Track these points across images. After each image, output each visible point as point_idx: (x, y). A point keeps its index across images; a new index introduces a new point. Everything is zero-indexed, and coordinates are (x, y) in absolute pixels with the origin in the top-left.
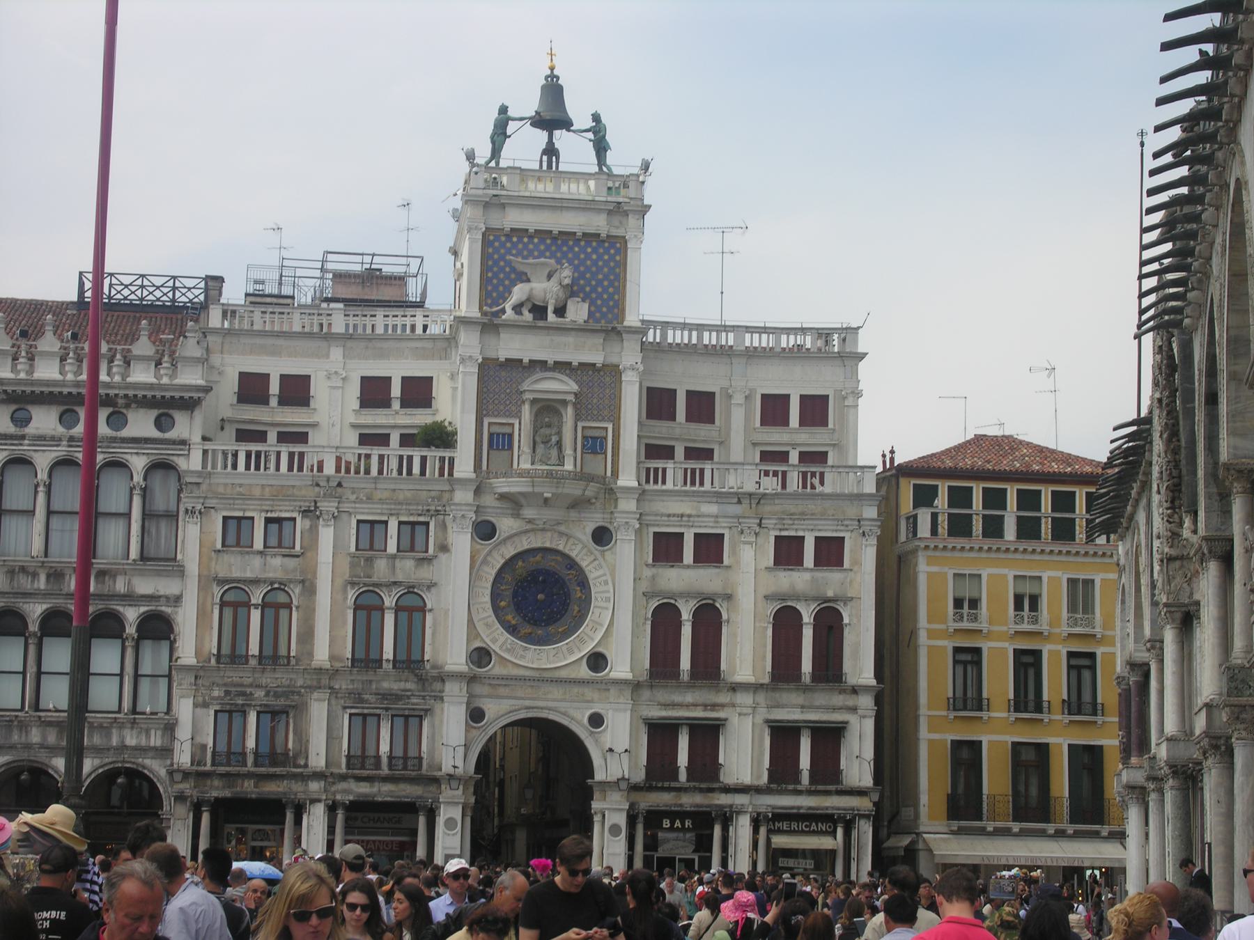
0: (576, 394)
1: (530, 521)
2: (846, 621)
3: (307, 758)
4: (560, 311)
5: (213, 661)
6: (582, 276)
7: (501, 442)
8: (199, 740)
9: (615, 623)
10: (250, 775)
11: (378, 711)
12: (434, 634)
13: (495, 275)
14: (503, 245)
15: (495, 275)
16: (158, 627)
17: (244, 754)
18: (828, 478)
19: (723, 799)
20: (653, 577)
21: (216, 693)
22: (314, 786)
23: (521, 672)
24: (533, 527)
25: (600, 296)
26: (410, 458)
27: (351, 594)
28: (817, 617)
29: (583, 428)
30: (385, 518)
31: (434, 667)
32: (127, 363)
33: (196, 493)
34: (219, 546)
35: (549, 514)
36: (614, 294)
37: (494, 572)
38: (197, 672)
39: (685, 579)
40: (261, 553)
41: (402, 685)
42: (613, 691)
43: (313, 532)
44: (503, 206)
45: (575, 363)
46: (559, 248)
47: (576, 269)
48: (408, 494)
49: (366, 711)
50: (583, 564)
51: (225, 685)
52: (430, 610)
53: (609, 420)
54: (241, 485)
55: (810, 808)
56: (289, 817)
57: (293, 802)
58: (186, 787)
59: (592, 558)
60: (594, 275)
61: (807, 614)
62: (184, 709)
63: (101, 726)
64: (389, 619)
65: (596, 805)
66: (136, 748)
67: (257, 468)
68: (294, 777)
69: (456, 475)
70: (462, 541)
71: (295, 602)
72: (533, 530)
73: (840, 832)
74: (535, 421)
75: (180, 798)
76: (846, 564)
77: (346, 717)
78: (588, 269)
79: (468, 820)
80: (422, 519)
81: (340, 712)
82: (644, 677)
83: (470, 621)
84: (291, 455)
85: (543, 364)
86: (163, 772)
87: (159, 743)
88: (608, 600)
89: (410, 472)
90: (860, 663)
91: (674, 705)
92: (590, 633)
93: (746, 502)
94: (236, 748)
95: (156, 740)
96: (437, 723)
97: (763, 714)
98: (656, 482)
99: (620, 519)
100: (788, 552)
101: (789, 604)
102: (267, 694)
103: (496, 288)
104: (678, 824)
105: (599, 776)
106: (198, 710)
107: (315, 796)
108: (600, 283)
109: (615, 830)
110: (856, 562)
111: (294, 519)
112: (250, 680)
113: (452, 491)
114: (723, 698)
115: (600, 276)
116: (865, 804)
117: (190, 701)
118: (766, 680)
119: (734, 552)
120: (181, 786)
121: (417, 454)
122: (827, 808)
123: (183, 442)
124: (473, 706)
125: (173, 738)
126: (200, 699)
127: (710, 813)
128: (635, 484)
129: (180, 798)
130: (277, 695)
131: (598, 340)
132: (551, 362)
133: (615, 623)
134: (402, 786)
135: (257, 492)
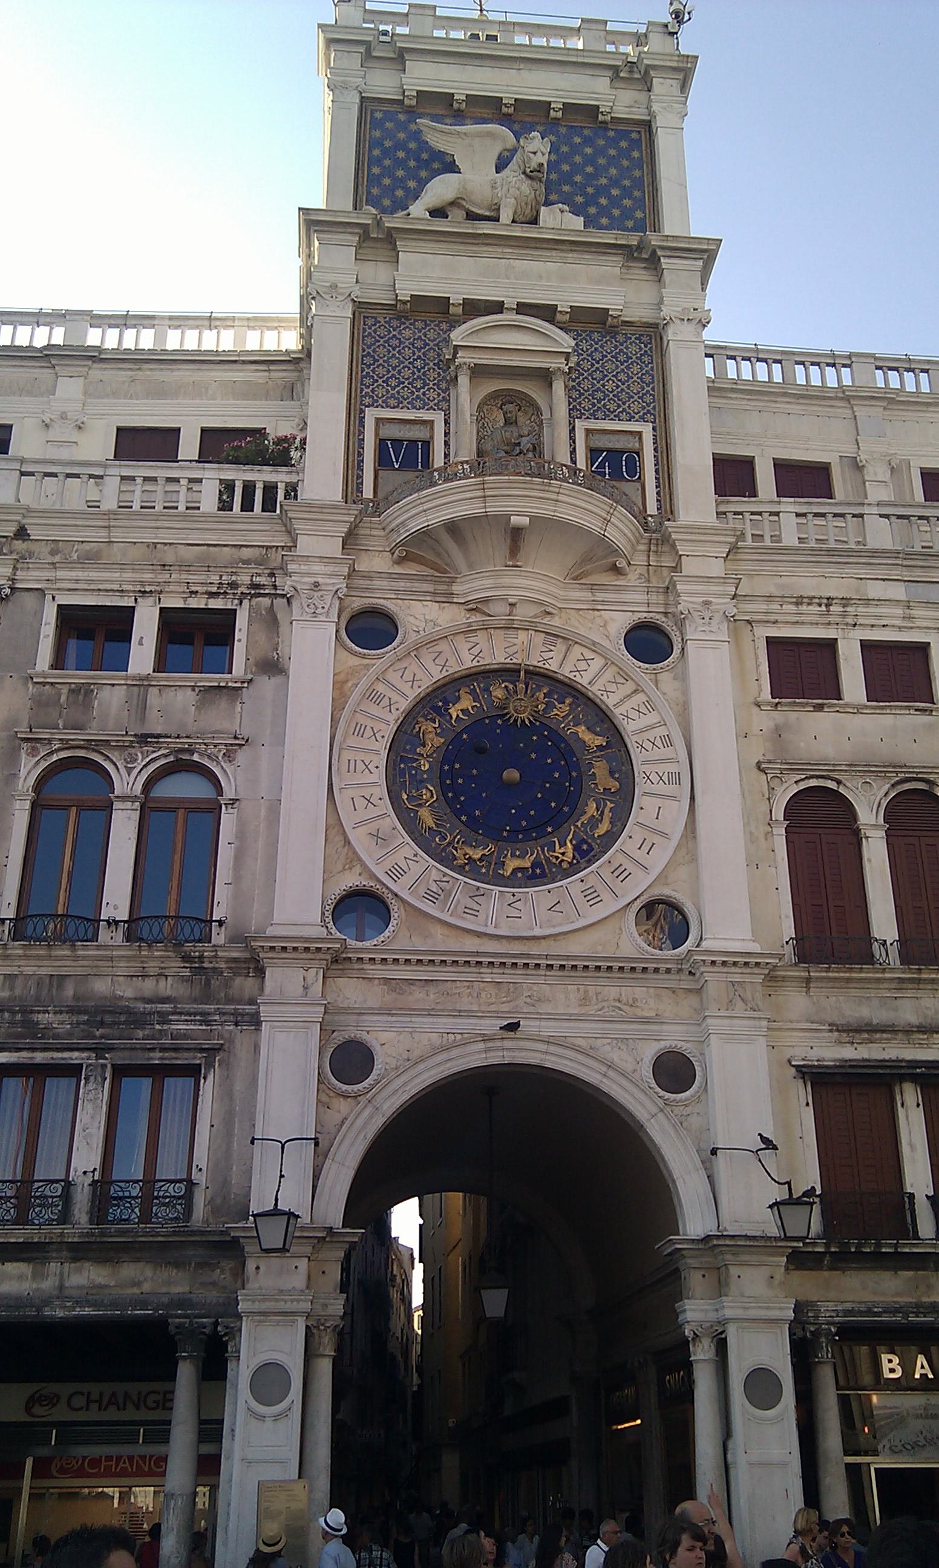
0: (567, 355)
1: (476, 607)
11: (75, 1057)
15: (389, 172)
20: (778, 732)
29: (588, 431)
36: (633, 210)
41: (148, 987)
44: (400, 58)
49: (39, 1057)
50: (610, 701)
53: (643, 419)
59: (630, 686)
70: (313, 645)
74: (480, 419)
78: (576, 169)
79: (324, 1368)
80: (216, 604)
83: (335, 825)
92: (639, 855)
96: (239, 1086)
99: (689, 596)
105: (695, 1222)
109: (763, 1389)
115: (604, 181)
124: (339, 1038)
134: (129, 1271)
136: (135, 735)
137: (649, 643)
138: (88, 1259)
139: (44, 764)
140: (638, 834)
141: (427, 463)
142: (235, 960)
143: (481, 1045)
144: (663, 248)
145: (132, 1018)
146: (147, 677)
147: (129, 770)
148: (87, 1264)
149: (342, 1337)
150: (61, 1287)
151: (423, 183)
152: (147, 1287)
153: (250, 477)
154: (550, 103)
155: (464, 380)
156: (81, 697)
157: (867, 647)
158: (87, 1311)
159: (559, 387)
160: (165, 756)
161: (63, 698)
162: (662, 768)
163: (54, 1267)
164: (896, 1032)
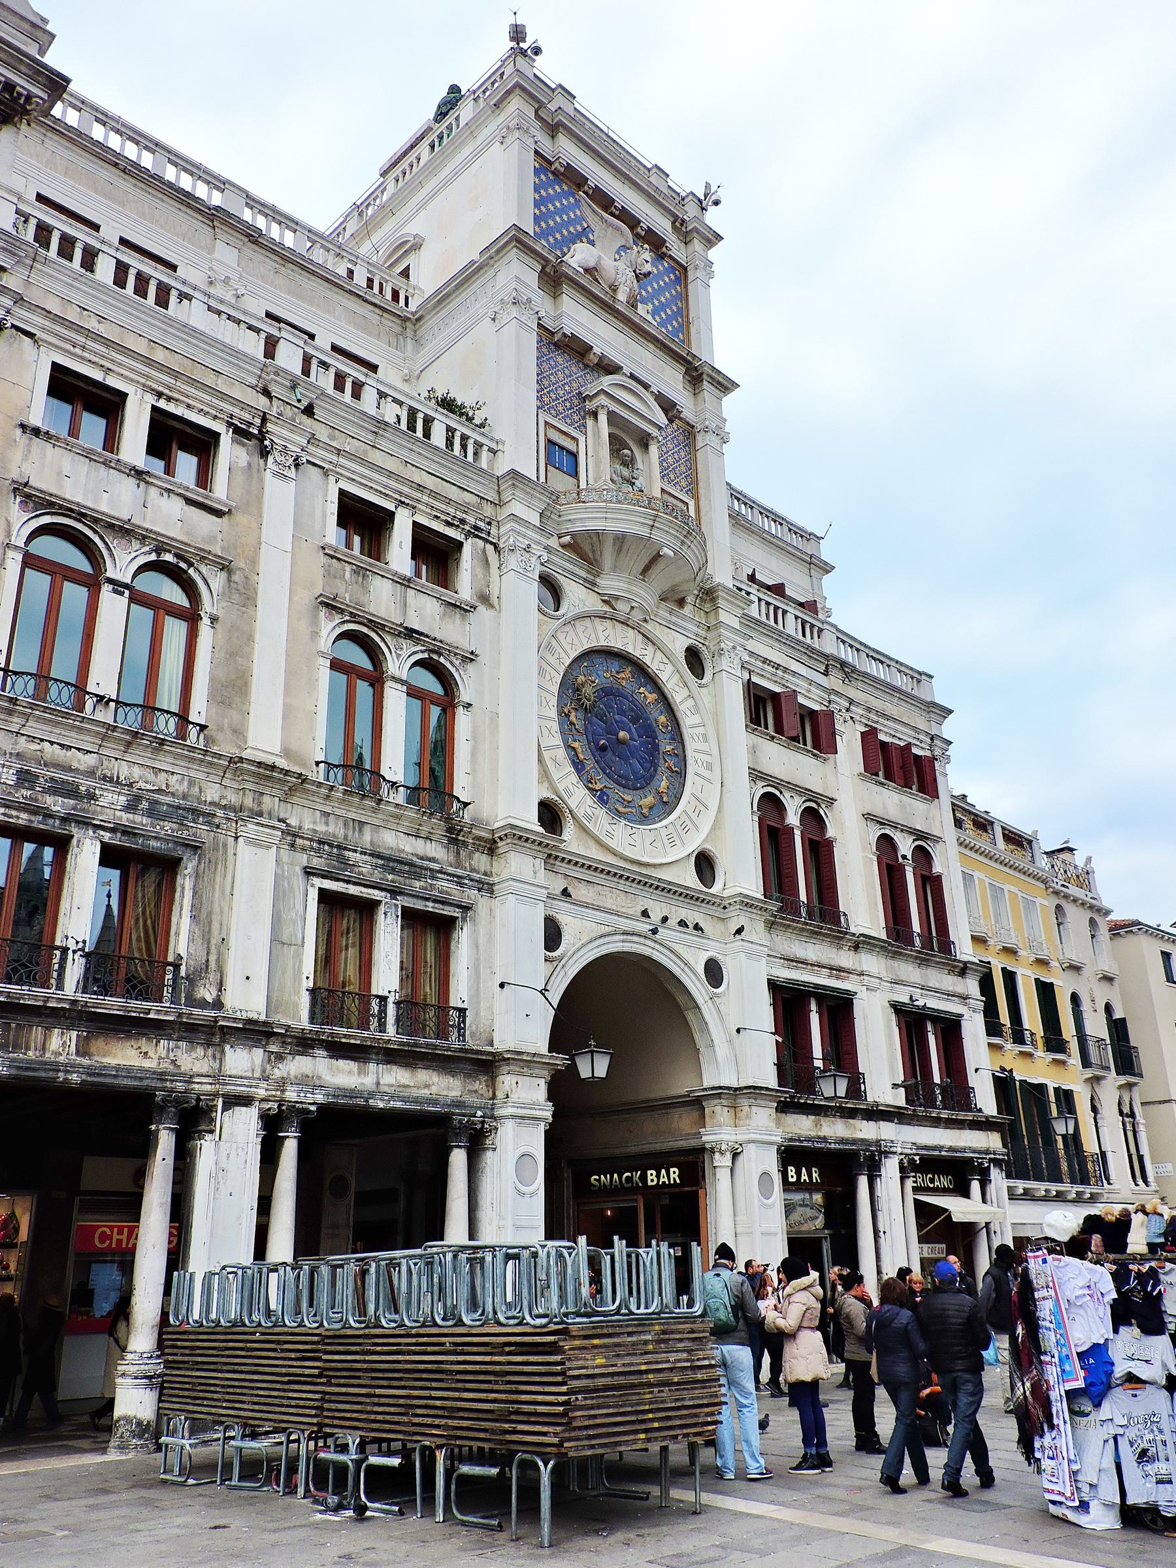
3: (221, 987)
7: (562, 457)
11: (376, 894)
12: (474, 754)
19: (866, 1130)
22: (241, 1061)
24: (610, 610)
30: (390, 506)
35: (644, 594)
45: (654, 389)
49: (353, 890)
51: (18, 755)
52: (468, 706)
55: (951, 1149)
56: (166, 1142)
57: (177, 1102)
59: (685, 692)
71: (208, 606)
73: (975, 1186)
77: (313, 895)
81: (299, 880)
96: (482, 940)
101: (888, 832)
102: (131, 807)
112: (91, 760)
122: (964, 1150)
127: (854, 1154)
136: (406, 628)
138: (395, 1064)
139: (338, 631)
140: (694, 802)
142: (479, 838)
143: (622, 937)
144: (709, 375)
145: (413, 868)
146: (409, 580)
147: (398, 656)
148: (394, 1067)
150: (378, 1084)
152: (434, 1090)
153: (468, 432)
154: (640, 221)
155: (603, 418)
156: (360, 579)
158: (399, 1105)
160: (422, 652)
161: (347, 575)
162: (703, 757)
163: (372, 1066)
164: (807, 964)
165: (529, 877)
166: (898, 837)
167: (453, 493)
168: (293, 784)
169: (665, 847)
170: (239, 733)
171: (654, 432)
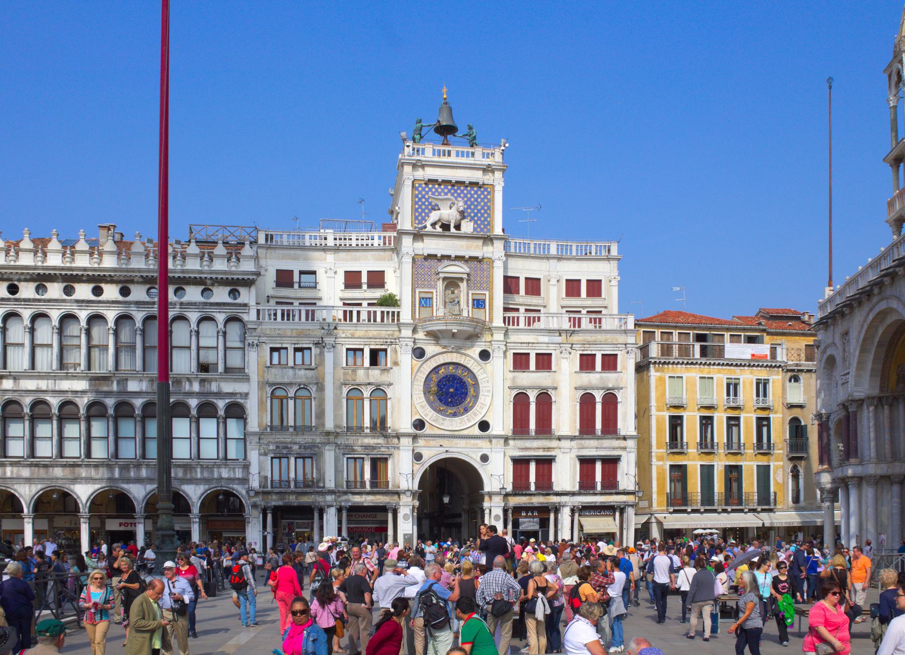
2: (619, 400)
4: (458, 227)
5: (268, 429)
6: (469, 207)
7: (426, 302)
8: (263, 474)
9: (494, 402)
10: (292, 493)
13: (420, 207)
14: (424, 189)
15: (420, 207)
16: (236, 411)
17: (289, 481)
18: (603, 321)
20: (514, 378)
21: (272, 447)
22: (329, 498)
23: (442, 432)
25: (479, 219)
26: (375, 312)
27: (345, 390)
28: (605, 398)
30: (361, 347)
31: (393, 431)
32: (211, 259)
33: (254, 334)
34: (268, 364)
37: (425, 377)
38: (260, 435)
39: (532, 379)
40: (292, 368)
42: (494, 441)
43: (322, 354)
44: (423, 166)
45: (467, 257)
46: (456, 191)
47: (466, 203)
48: (375, 333)
50: (475, 371)
54: (279, 329)
56: (316, 515)
58: (258, 500)
60: (476, 206)
61: (599, 396)
62: (254, 456)
63: (207, 467)
64: (367, 404)
65: (486, 504)
66: (228, 479)
67: (288, 319)
68: (318, 493)
69: (401, 321)
72: (445, 352)
75: (255, 506)
76: (619, 369)
77: (345, 459)
78: (472, 203)
80: (383, 347)
81: (341, 457)
82: (510, 434)
84: (307, 311)
85: (448, 257)
86: (244, 492)
87: (240, 476)
88: (489, 391)
89: (375, 321)
90: (626, 422)
91: (526, 449)
93: (564, 335)
94: (284, 478)
95: (239, 474)
97: (575, 453)
98: (513, 325)
100: (587, 363)
103: (420, 214)
104: (530, 514)
105: (487, 489)
106: (262, 457)
107: (329, 504)
108: (479, 211)
110: (625, 368)
111: (310, 349)
113: (400, 331)
114: (554, 443)
116: (630, 499)
117: (257, 452)
118: (577, 434)
119: (557, 365)
120: (255, 499)
121: (379, 310)
123: (245, 305)
125: (249, 473)
126: (262, 451)
127: (548, 507)
128: (503, 325)
129: (255, 506)
130: (305, 448)
131: (480, 242)
132: (453, 256)
133: (494, 402)
135: (289, 333)
137: (485, 355)
141: (431, 306)
149: (418, 509)
151: (430, 212)
155: (441, 281)
157: (537, 354)
159: (465, 282)
165: (407, 444)
166: (594, 393)
167: (383, 334)
168: (337, 435)
169: (467, 422)
170: (323, 425)
171: (465, 276)
